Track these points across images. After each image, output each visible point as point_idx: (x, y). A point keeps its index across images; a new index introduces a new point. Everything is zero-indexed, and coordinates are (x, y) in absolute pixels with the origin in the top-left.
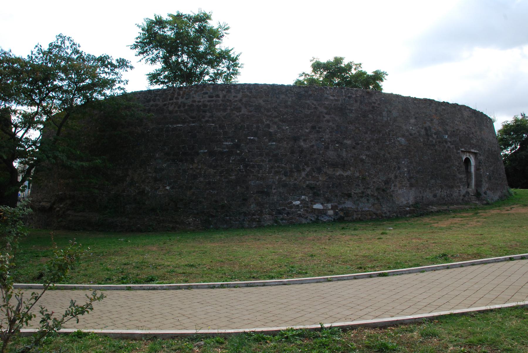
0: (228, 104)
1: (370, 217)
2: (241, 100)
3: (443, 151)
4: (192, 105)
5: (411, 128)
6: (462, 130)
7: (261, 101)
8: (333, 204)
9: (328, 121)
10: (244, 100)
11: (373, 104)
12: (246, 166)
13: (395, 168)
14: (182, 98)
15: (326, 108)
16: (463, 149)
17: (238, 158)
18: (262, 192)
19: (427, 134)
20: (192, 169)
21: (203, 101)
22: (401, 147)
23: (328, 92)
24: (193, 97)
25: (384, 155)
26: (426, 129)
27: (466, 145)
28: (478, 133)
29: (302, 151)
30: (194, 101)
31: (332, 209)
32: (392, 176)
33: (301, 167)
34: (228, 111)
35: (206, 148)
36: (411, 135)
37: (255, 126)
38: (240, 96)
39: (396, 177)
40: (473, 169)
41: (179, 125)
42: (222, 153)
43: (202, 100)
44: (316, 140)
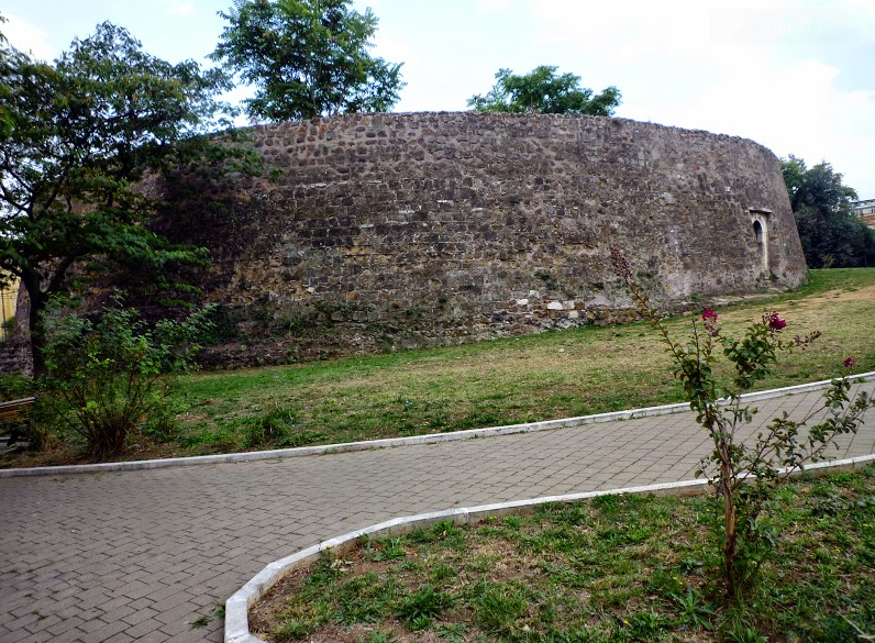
0: (401, 146)
1: (631, 319)
2: (421, 140)
4: (339, 151)
7: (453, 141)
9: (560, 171)
10: (427, 139)
11: (624, 141)
12: (440, 247)
14: (321, 138)
15: (555, 149)
16: (752, 208)
17: (426, 234)
18: (469, 287)
19: (701, 186)
20: (350, 256)
21: (359, 144)
23: (556, 123)
24: (340, 137)
27: (755, 202)
28: (769, 182)
29: (523, 220)
30: (342, 144)
31: (575, 309)
32: (658, 253)
33: (525, 245)
34: (403, 159)
35: (371, 222)
37: (447, 182)
38: (419, 133)
39: (664, 255)
40: (764, 239)
41: (321, 185)
42: (398, 228)
43: (355, 141)
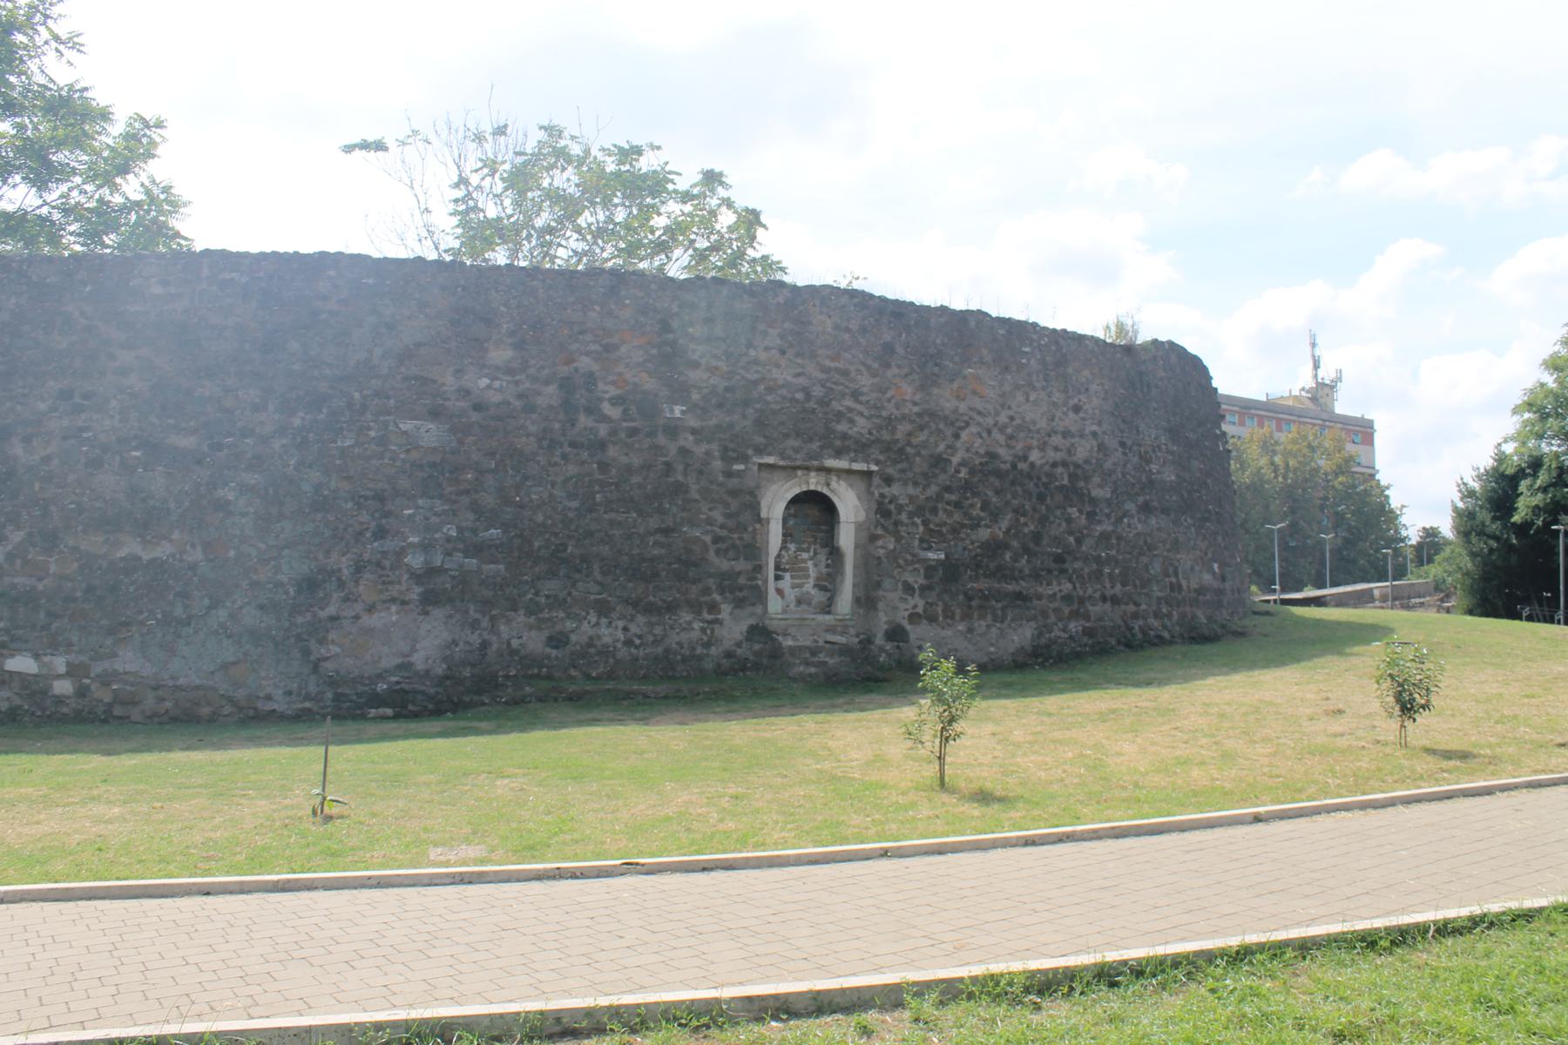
3: (647, 467)
5: (484, 382)
6: (786, 385)
8: (72, 657)
13: (361, 533)
16: (771, 460)
22: (414, 455)
25: (318, 488)
26: (567, 385)
31: (68, 674)
36: (477, 407)
39: (359, 568)
40: (846, 538)
44: (65, 438)
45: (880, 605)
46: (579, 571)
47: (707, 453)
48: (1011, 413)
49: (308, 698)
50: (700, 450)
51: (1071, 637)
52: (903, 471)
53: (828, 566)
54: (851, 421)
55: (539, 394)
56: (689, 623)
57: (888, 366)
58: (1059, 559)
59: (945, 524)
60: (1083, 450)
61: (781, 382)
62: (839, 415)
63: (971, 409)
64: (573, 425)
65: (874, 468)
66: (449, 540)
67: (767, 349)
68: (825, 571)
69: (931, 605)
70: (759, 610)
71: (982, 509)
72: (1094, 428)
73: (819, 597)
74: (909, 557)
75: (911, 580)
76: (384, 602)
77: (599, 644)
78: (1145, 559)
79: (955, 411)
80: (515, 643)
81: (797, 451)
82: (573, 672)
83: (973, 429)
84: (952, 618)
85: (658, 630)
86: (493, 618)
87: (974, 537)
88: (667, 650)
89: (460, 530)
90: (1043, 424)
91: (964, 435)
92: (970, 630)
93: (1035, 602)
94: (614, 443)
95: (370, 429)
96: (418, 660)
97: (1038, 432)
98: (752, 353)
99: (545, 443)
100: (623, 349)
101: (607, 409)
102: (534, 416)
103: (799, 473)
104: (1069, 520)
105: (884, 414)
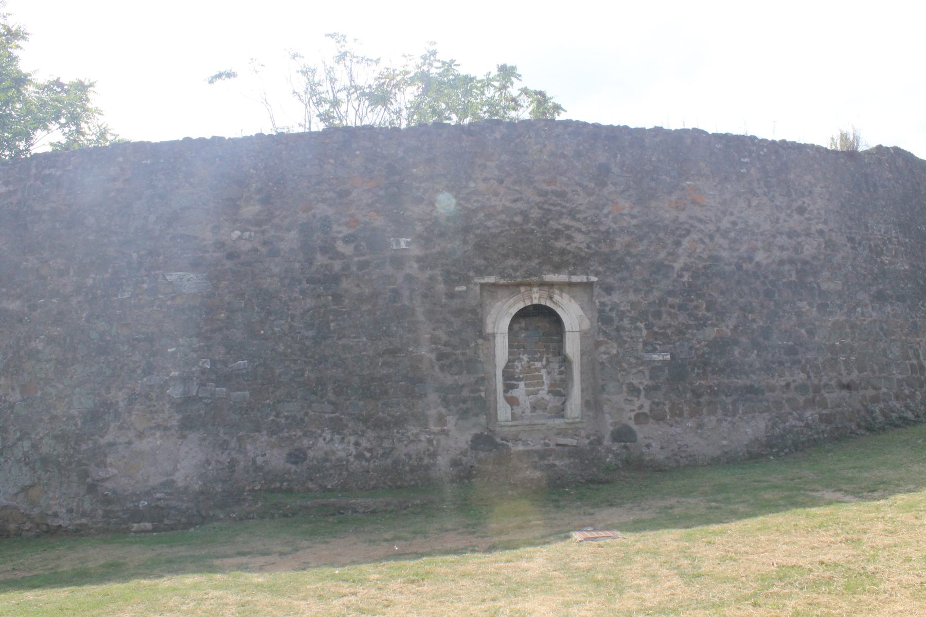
13: (134, 371)
16: (491, 280)
22: (178, 301)
32: (119, 397)
36: (231, 256)
39: (131, 401)
40: (572, 347)
45: (606, 408)
46: (315, 393)
47: (431, 278)
48: (733, 218)
49: (84, 515)
50: (425, 276)
51: (807, 425)
52: (623, 279)
53: (561, 373)
54: (569, 238)
55: (282, 239)
56: (417, 435)
57: (603, 184)
58: (791, 351)
59: (670, 326)
60: (809, 249)
61: (500, 208)
62: (558, 232)
63: (691, 218)
64: (311, 264)
65: (594, 279)
66: (203, 372)
67: (485, 180)
68: (558, 377)
69: (658, 404)
70: (483, 419)
71: (708, 310)
72: (820, 226)
73: (553, 402)
74: (632, 360)
75: (635, 382)
76: (151, 428)
77: (333, 458)
78: (882, 345)
79: (675, 220)
80: (259, 460)
81: (516, 269)
82: (310, 485)
83: (695, 236)
84: (681, 415)
85: (387, 444)
86: (239, 439)
87: (700, 337)
88: (396, 462)
89: (213, 363)
90: (767, 226)
91: (685, 242)
92: (700, 426)
93: (767, 394)
94: (347, 277)
95: (143, 282)
96: (179, 478)
97: (762, 234)
98: (472, 184)
99: (287, 281)
100: (354, 194)
101: (341, 247)
102: (277, 259)
103: (522, 289)
104: (799, 314)
105: (602, 228)
